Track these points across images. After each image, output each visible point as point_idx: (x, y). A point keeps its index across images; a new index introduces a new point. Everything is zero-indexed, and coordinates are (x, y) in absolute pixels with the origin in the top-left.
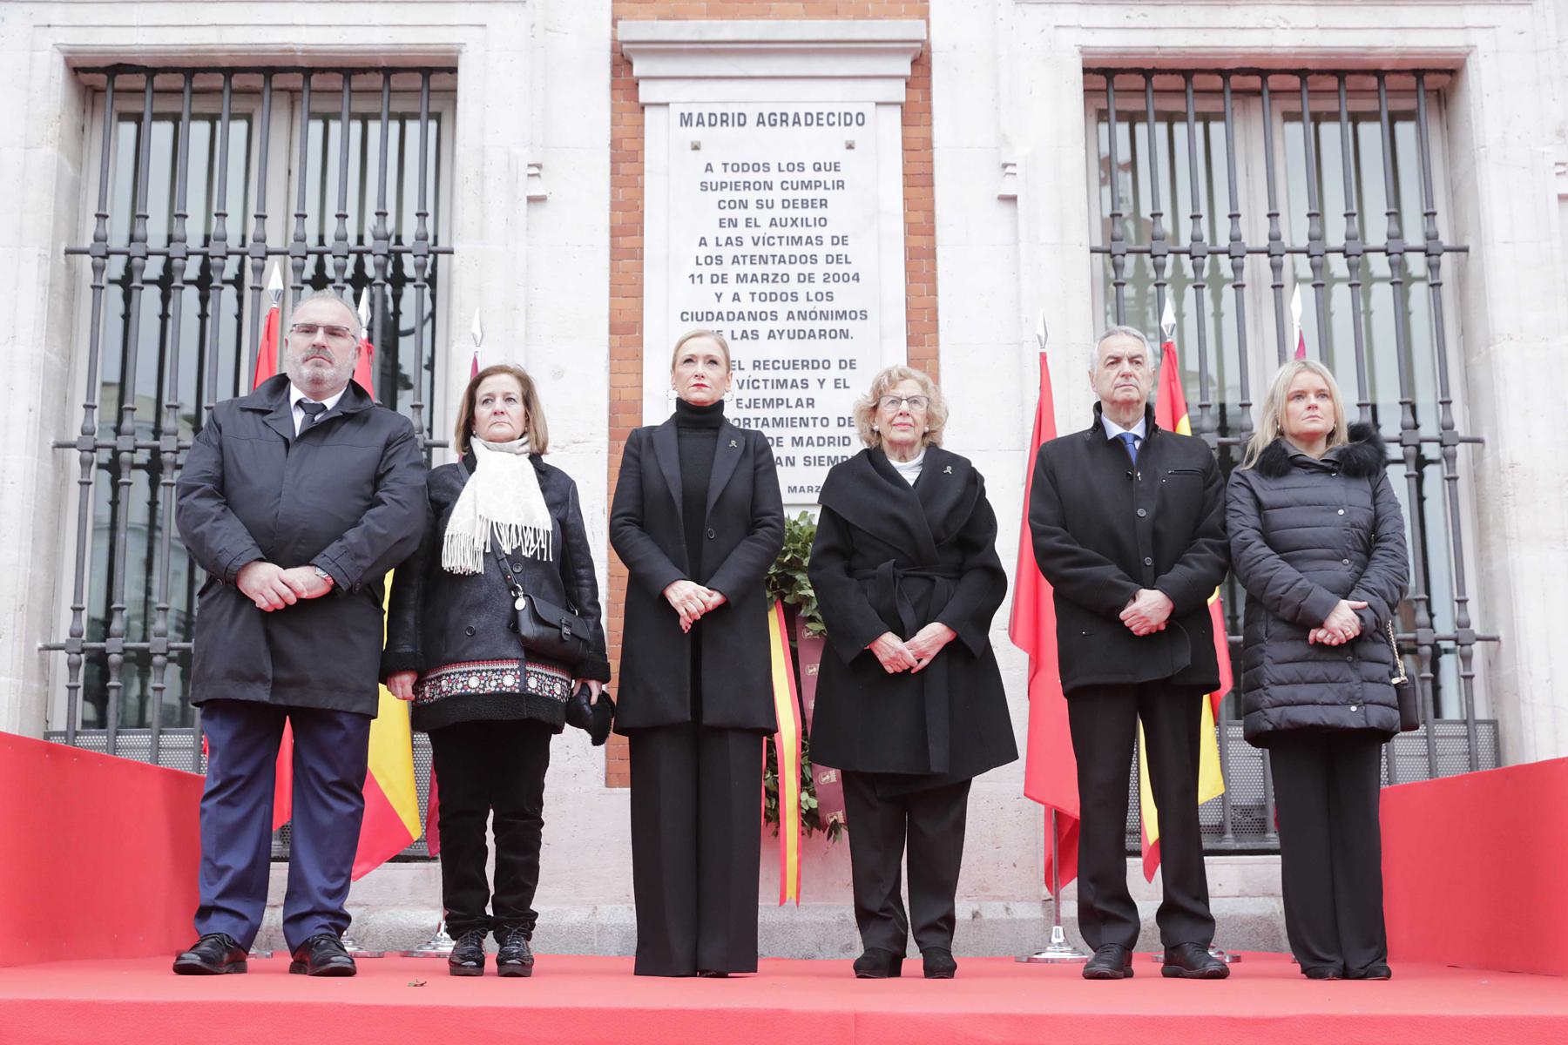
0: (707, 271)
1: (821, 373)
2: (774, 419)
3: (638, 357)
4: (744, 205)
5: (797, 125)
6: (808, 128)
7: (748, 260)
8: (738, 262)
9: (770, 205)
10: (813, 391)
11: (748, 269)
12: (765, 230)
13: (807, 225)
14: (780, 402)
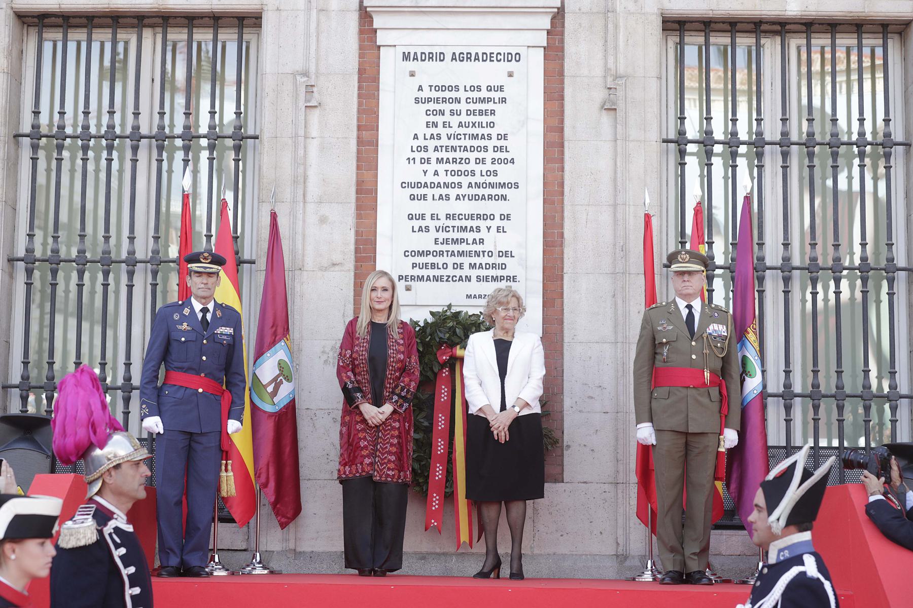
0: (418, 156)
1: (489, 223)
2: (458, 251)
3: (375, 209)
4: (442, 113)
5: (477, 61)
6: (484, 63)
7: (444, 149)
8: (438, 151)
9: (459, 113)
10: (483, 234)
11: (444, 155)
12: (456, 129)
13: (482, 127)
14: (462, 241)
